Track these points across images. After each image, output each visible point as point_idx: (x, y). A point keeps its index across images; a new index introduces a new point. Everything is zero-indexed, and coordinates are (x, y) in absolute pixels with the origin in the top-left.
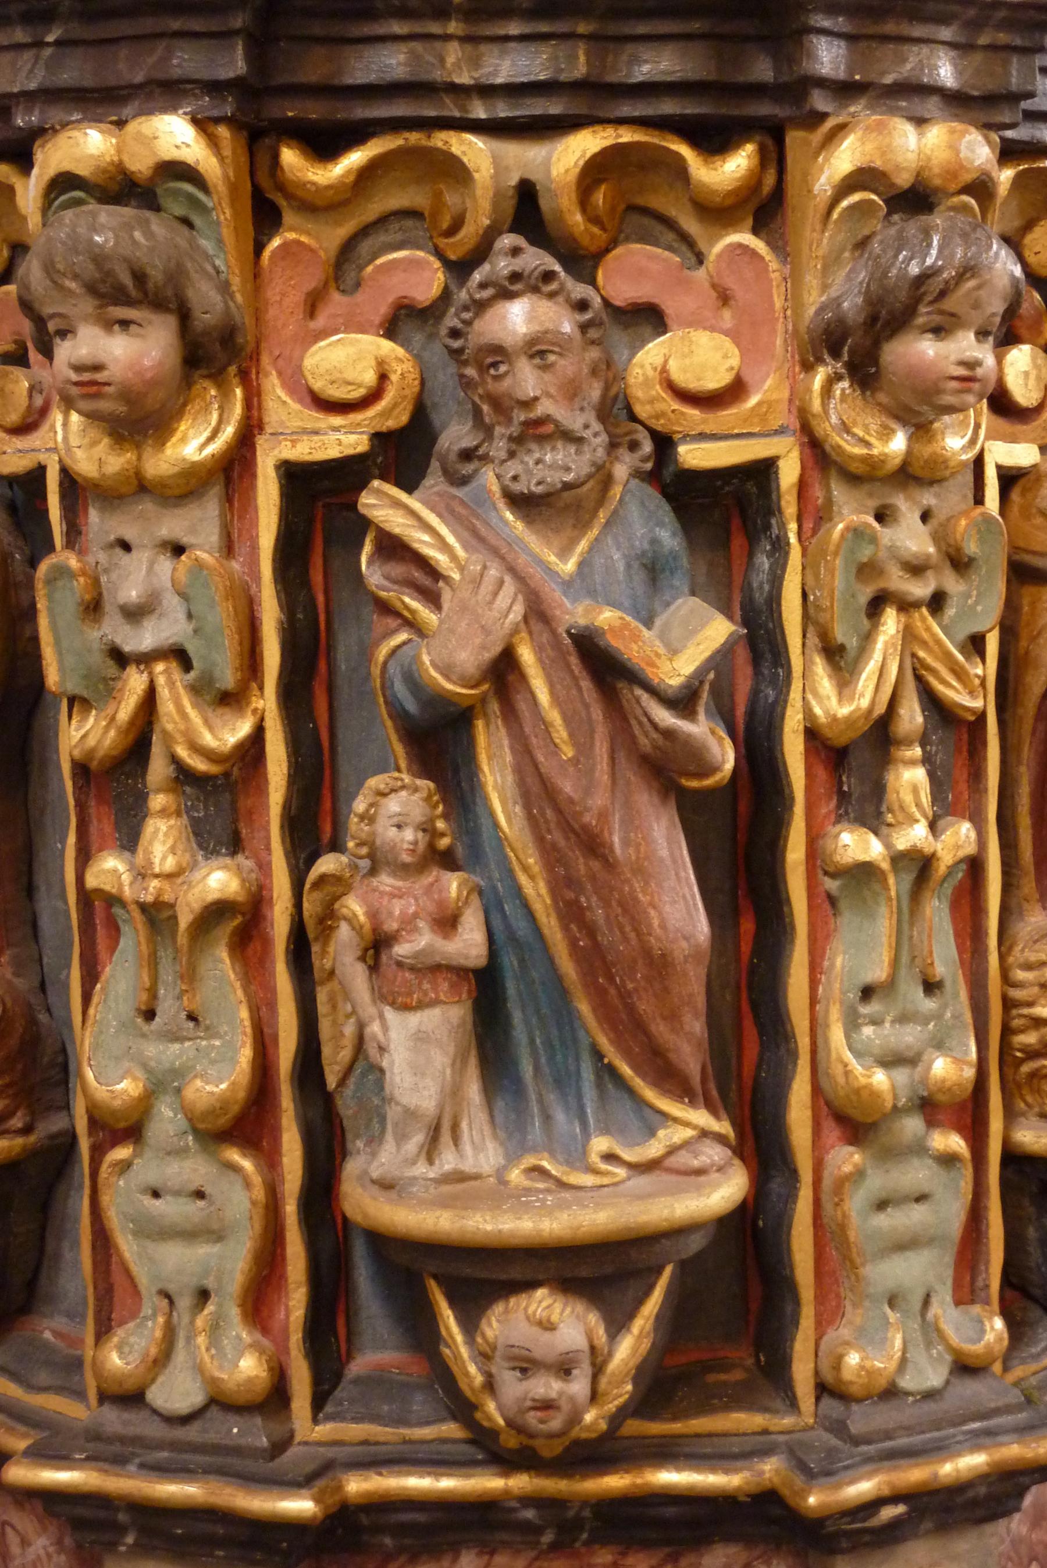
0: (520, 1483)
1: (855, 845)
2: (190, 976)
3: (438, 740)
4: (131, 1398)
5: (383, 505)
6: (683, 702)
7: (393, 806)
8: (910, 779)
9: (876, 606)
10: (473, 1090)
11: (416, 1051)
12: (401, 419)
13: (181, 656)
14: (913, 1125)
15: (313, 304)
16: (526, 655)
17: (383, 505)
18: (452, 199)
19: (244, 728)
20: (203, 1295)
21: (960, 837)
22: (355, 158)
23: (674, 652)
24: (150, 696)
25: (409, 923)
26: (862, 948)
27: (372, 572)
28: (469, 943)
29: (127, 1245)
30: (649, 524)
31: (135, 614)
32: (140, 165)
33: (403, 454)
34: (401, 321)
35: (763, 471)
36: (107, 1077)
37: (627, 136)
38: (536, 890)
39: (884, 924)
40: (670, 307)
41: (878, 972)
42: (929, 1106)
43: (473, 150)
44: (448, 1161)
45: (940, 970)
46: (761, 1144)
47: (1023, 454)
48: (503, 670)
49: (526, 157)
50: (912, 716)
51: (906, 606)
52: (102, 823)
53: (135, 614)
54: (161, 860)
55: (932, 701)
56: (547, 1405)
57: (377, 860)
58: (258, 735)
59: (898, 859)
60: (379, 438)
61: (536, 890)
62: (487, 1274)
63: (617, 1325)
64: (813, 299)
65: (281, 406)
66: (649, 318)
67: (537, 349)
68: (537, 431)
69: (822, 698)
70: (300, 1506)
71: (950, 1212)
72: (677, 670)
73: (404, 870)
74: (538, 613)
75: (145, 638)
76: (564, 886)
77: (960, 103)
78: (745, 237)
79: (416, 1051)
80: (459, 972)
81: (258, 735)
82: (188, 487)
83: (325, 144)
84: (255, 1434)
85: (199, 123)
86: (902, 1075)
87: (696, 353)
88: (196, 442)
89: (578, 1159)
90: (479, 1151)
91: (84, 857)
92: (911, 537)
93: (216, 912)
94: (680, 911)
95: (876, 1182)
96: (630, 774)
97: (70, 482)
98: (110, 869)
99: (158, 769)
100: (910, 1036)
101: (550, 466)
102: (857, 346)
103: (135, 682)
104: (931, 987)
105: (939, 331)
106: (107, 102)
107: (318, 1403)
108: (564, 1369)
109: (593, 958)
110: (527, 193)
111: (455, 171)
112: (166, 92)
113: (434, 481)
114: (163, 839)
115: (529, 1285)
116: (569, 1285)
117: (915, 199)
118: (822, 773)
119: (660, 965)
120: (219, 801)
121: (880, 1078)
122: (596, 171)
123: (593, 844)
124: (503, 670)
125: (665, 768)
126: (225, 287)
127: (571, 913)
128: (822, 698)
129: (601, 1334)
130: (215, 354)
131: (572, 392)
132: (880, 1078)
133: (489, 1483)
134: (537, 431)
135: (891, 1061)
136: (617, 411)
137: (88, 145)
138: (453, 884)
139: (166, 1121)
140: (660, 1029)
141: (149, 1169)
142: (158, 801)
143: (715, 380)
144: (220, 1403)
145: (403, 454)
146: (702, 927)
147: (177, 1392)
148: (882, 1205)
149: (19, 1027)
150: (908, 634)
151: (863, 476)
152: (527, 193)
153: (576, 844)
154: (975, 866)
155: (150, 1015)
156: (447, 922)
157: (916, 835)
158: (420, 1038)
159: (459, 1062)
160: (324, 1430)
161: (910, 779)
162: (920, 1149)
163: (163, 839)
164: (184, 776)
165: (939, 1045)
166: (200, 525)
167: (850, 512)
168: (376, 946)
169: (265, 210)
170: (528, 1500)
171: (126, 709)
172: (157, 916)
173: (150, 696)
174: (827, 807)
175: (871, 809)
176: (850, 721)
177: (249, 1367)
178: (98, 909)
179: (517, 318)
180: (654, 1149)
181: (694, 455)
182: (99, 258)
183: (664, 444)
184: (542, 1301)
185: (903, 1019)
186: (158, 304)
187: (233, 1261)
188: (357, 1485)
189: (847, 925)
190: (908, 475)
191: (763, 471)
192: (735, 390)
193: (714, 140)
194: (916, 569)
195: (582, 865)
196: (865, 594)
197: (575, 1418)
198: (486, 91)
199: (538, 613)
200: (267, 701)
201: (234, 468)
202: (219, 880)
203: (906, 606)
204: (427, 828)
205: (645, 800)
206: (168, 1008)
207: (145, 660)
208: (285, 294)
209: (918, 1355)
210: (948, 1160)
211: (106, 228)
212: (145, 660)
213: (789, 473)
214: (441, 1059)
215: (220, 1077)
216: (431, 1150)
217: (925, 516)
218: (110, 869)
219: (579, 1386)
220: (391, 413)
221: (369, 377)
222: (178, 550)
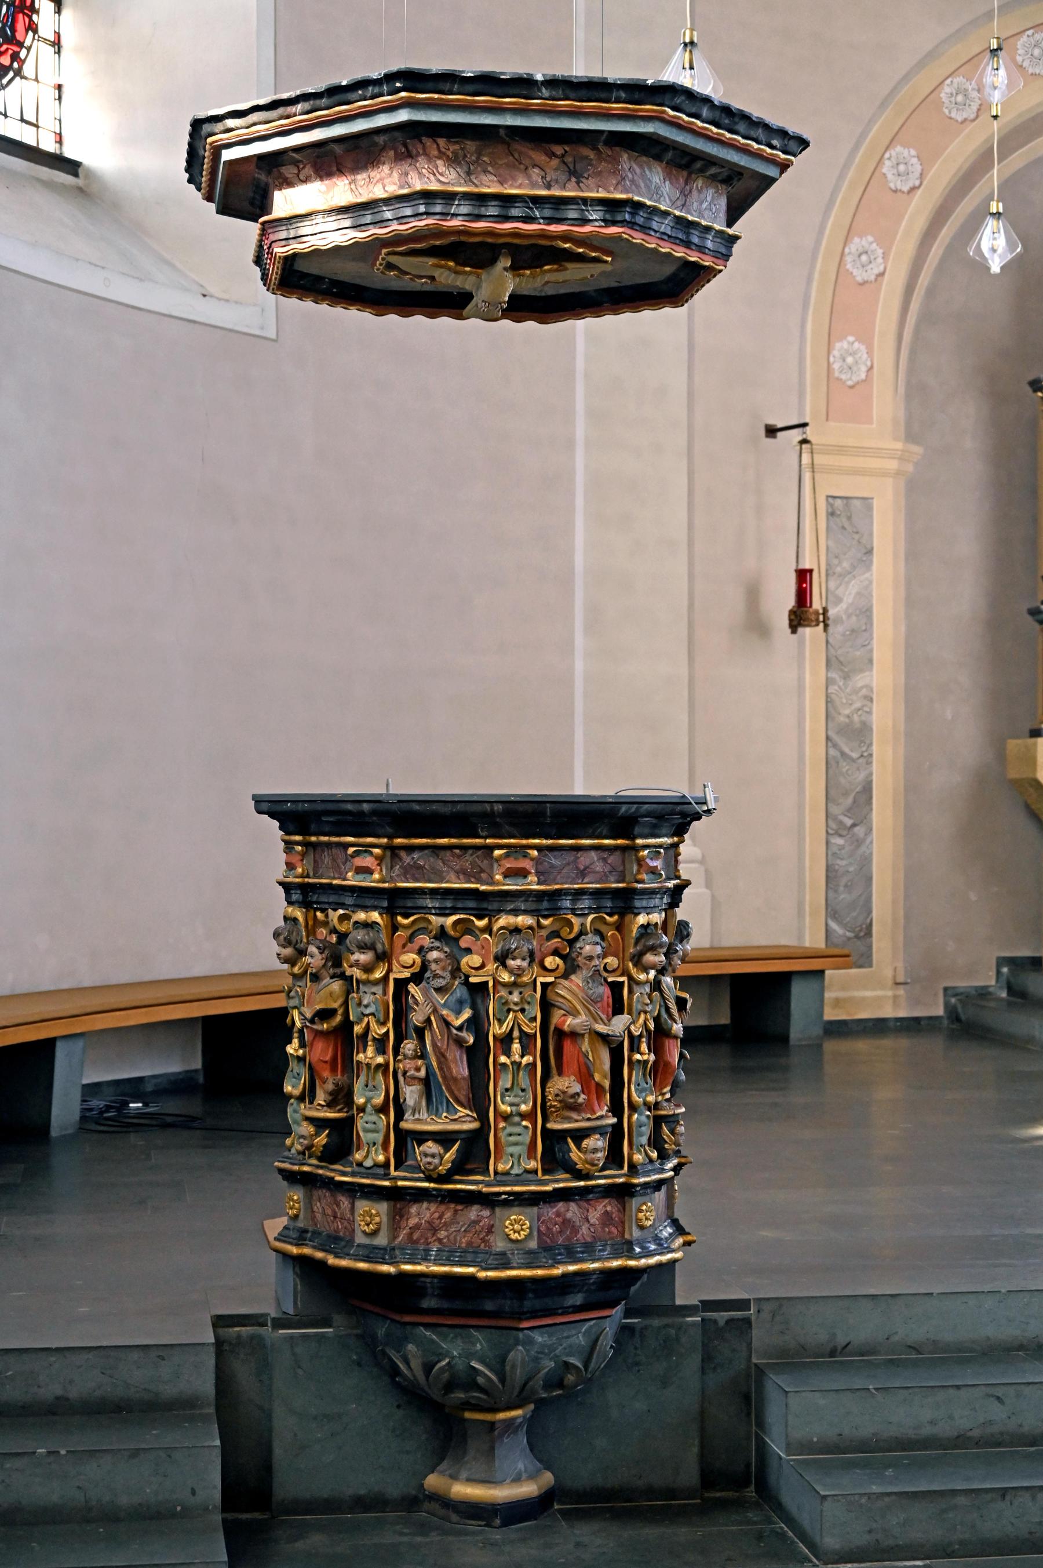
0: (432, 1185)
1: (503, 1059)
2: (374, 1078)
3: (420, 1033)
4: (360, 1164)
5: (412, 988)
6: (460, 1028)
7: (409, 1046)
8: (516, 1046)
9: (509, 1011)
10: (424, 1103)
11: (411, 1094)
12: (417, 970)
13: (373, 1014)
14: (517, 1119)
15: (404, 946)
16: (433, 1018)
17: (412, 988)
18: (430, 927)
19: (385, 1030)
20: (374, 1144)
21: (526, 1060)
22: (412, 919)
23: (457, 1019)
24: (368, 1022)
25: (410, 1069)
26: (506, 1081)
27: (410, 1001)
28: (422, 1073)
29: (361, 1134)
30: (460, 992)
31: (366, 1006)
32: (369, 921)
33: (417, 978)
34: (421, 951)
35: (487, 982)
36: (360, 1100)
37: (462, 916)
38: (435, 1064)
39: (510, 1076)
40: (473, 948)
41: (508, 1086)
42: (523, 1116)
43: (433, 918)
44: (417, 1116)
45: (523, 1087)
46: (483, 1118)
47: (551, 979)
48: (428, 1021)
49: (441, 920)
50: (516, 1034)
51: (515, 1011)
52: (361, 1048)
53: (366, 1006)
54: (368, 1055)
55: (521, 1030)
56: (429, 1163)
57: (405, 1057)
58: (388, 1031)
59: (513, 1063)
60: (412, 974)
61: (435, 1064)
62: (421, 1137)
63: (447, 1150)
64: (495, 950)
65: (396, 967)
66: (468, 951)
67: (436, 961)
68: (436, 976)
69: (496, 1030)
70: (387, 1183)
71: (527, 1138)
72: (458, 1023)
73: (410, 1059)
74: (435, 1011)
75: (367, 1012)
76: (439, 1063)
77: (525, 912)
78: (487, 936)
79: (411, 1094)
80: (420, 1079)
81: (388, 1031)
82: (376, 983)
83: (406, 916)
84: (381, 1171)
85: (380, 914)
86: (514, 1108)
87: (475, 960)
88: (378, 974)
89: (440, 1118)
90: (424, 1115)
91: (358, 1053)
92: (515, 997)
93: (379, 1066)
94: (461, 1069)
95: (509, 1130)
96: (451, 1041)
97: (358, 981)
98: (361, 1057)
99: (370, 1037)
100: (516, 1100)
101: (440, 982)
102: (502, 959)
103: (366, 1020)
104: (523, 1090)
105: (513, 959)
106: (365, 908)
107: (396, 1169)
108: (433, 1156)
109: (444, 1078)
110: (442, 927)
111: (429, 922)
112: (374, 908)
113: (424, 983)
114: (370, 1051)
115: (427, 1140)
116: (436, 1141)
117: (516, 930)
118: (498, 1044)
119: (455, 1079)
120: (381, 1045)
121: (509, 1109)
122: (456, 923)
123: (444, 1056)
124: (428, 1021)
125: (459, 1042)
126: (383, 944)
127: (441, 1069)
128: (496, 1030)
129: (442, 1151)
130: (384, 957)
131: (444, 969)
132: (509, 1109)
133: (426, 1185)
134: (436, 976)
135: (511, 1105)
136: (456, 971)
137: (361, 916)
138: (420, 1062)
139: (369, 1108)
140: (456, 1092)
141: (366, 1118)
142: (370, 1043)
143: (477, 965)
144: (376, 1165)
145: (417, 978)
146: (466, 1073)
147: (368, 1163)
148: (510, 1135)
149: (346, 1090)
150: (515, 1017)
151: (505, 985)
152: (442, 927)
153: (441, 1056)
154: (534, 1065)
155: (367, 1086)
156: (418, 1069)
157: (517, 1058)
158: (412, 1091)
159: (420, 1097)
160: (396, 1174)
161: (516, 1046)
162: (519, 1124)
163: (370, 1051)
164: (374, 1039)
165: (525, 1103)
166: (378, 990)
167: (503, 992)
168: (405, 1073)
169: (395, 927)
170: (434, 1189)
171: (364, 1025)
172: (368, 1065)
173: (368, 1022)
174: (500, 1051)
175: (508, 1053)
176: (501, 1034)
177: (381, 1158)
178: (359, 1063)
179: (434, 955)
180: (456, 1117)
181: (472, 980)
182: (358, 941)
183: (467, 977)
184: (430, 1143)
185: (515, 1096)
186: (370, 949)
187: (379, 1137)
188: (400, 1183)
189: (503, 1076)
190: (515, 984)
191: (487, 982)
192: (483, 966)
193: (480, 917)
194: (516, 1004)
195: (442, 1059)
196: (506, 1008)
197: (436, 1168)
198: (435, 908)
199: (435, 1011)
200: (390, 1025)
201: (385, 979)
202: (380, 1060)
203: (515, 1011)
204: (415, 1051)
205: (453, 1047)
206: (370, 1085)
207: (368, 1015)
208: (398, 943)
209: (516, 1167)
210: (526, 1127)
211: (360, 935)
212: (368, 1015)
213: (491, 984)
214: (416, 1096)
215: (379, 1100)
216: (413, 1114)
217: (521, 993)
218: (361, 1057)
219: (436, 1161)
220: (416, 969)
221: (411, 962)
222: (375, 994)
